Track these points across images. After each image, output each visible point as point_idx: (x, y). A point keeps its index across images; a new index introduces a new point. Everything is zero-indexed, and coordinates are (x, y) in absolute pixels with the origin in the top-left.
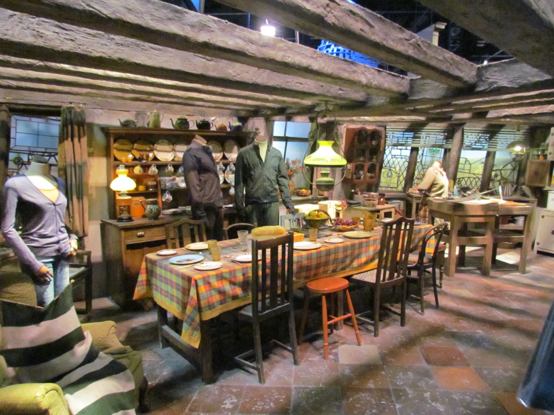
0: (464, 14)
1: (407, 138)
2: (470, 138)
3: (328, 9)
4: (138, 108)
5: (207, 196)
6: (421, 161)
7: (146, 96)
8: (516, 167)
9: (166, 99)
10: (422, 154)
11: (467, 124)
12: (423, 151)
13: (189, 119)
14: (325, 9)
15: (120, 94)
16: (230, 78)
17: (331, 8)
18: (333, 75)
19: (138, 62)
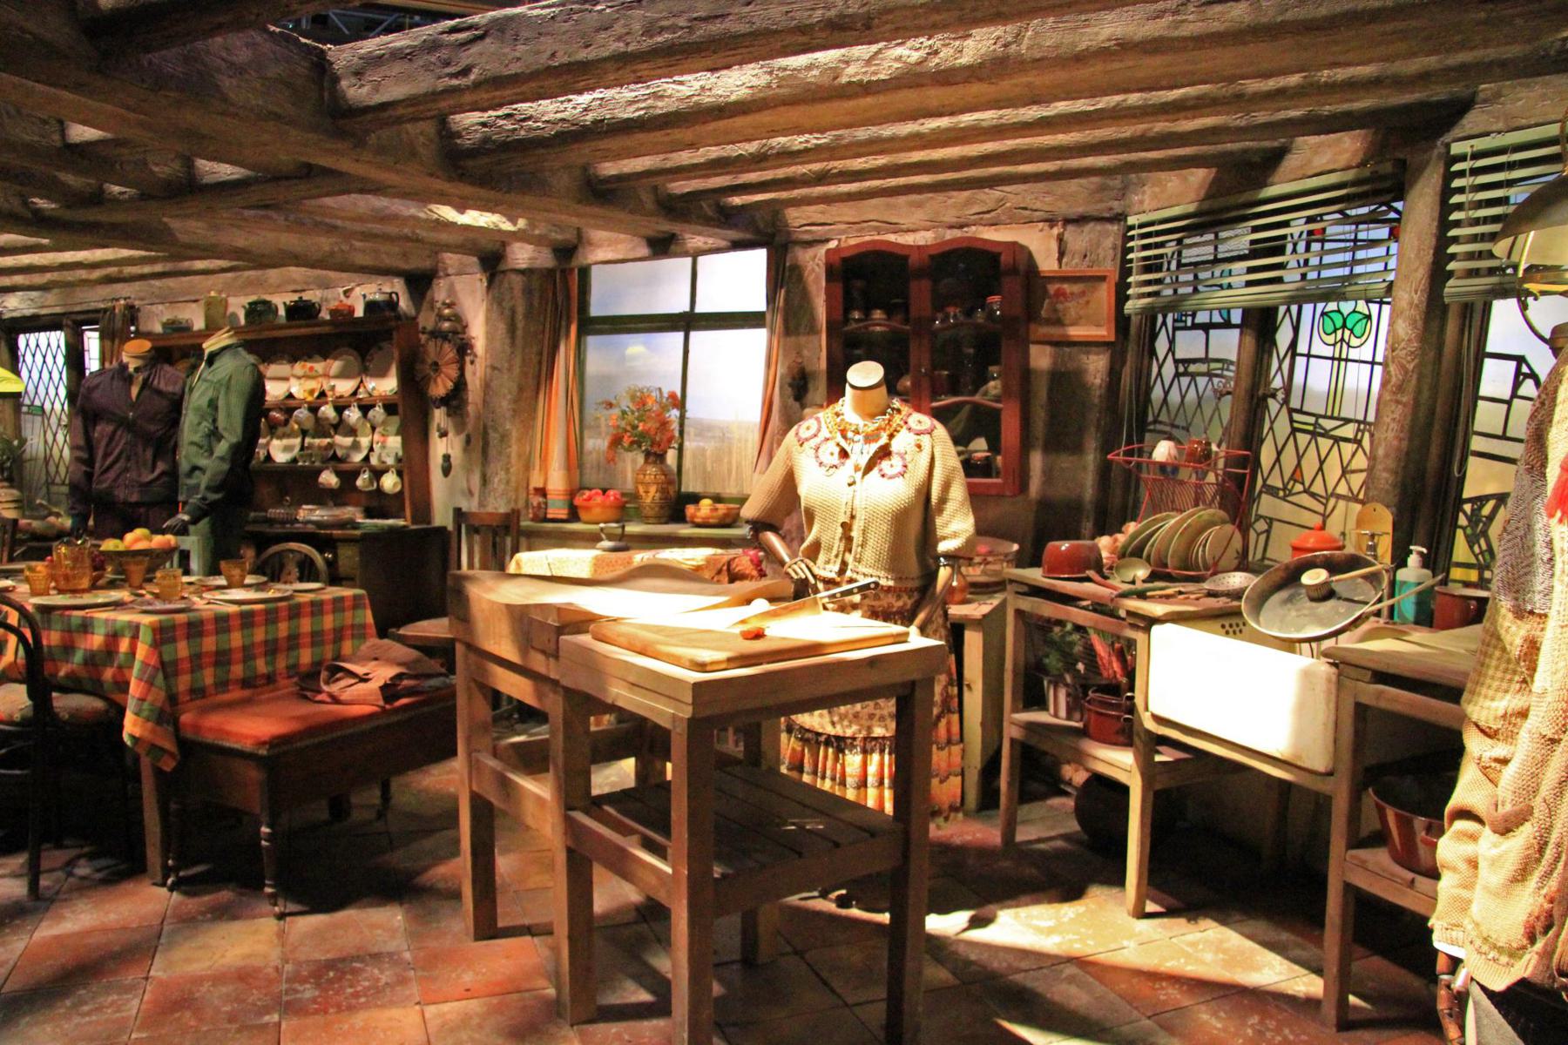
10: (1293, 345)
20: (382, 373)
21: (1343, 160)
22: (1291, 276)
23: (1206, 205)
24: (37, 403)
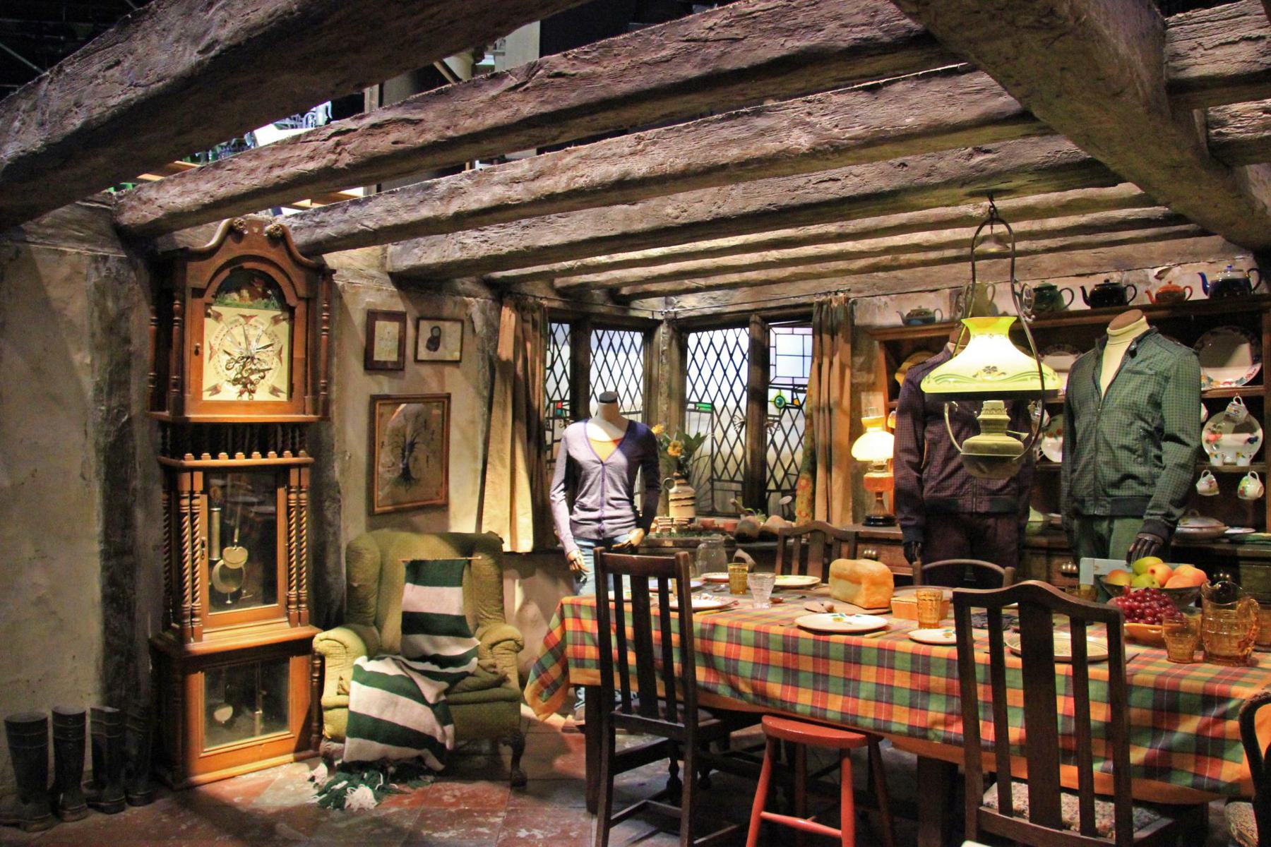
4: (956, 279)
5: (933, 478)
7: (889, 257)
9: (921, 256)
15: (842, 265)
16: (670, 223)
18: (692, 168)
19: (543, 244)
20: (1221, 361)
24: (706, 400)
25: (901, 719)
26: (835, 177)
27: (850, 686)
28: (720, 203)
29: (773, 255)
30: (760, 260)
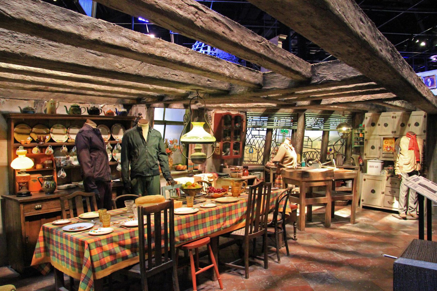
0: (299, 23)
1: (263, 121)
2: (310, 121)
3: (197, 16)
5: (97, 171)
6: (275, 140)
7: (44, 87)
8: (344, 143)
9: (61, 89)
10: (276, 134)
11: (307, 111)
12: (276, 132)
13: (81, 106)
14: (194, 15)
15: (21, 85)
16: (117, 70)
17: (199, 15)
18: (202, 68)
19: (38, 56)
21: (290, 111)
22: (275, 125)
23: (265, 113)
25: (216, 228)
26: (177, 74)
27: (204, 225)
28: (140, 70)
29: (29, 78)
30: (21, 78)
